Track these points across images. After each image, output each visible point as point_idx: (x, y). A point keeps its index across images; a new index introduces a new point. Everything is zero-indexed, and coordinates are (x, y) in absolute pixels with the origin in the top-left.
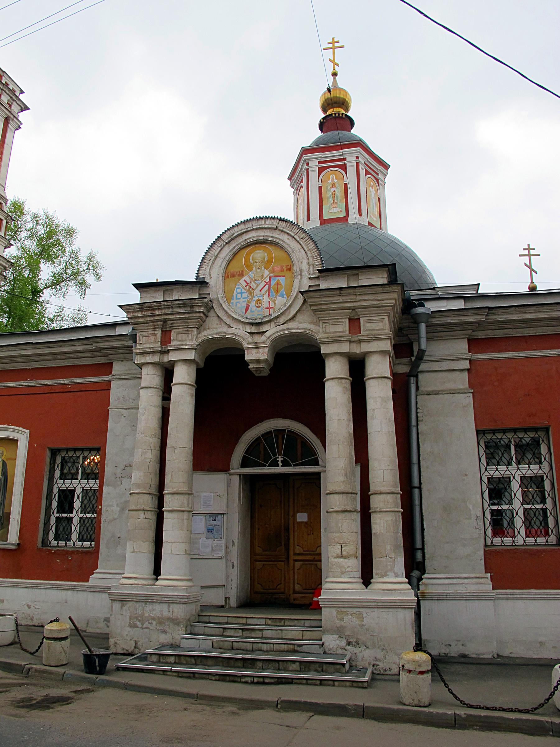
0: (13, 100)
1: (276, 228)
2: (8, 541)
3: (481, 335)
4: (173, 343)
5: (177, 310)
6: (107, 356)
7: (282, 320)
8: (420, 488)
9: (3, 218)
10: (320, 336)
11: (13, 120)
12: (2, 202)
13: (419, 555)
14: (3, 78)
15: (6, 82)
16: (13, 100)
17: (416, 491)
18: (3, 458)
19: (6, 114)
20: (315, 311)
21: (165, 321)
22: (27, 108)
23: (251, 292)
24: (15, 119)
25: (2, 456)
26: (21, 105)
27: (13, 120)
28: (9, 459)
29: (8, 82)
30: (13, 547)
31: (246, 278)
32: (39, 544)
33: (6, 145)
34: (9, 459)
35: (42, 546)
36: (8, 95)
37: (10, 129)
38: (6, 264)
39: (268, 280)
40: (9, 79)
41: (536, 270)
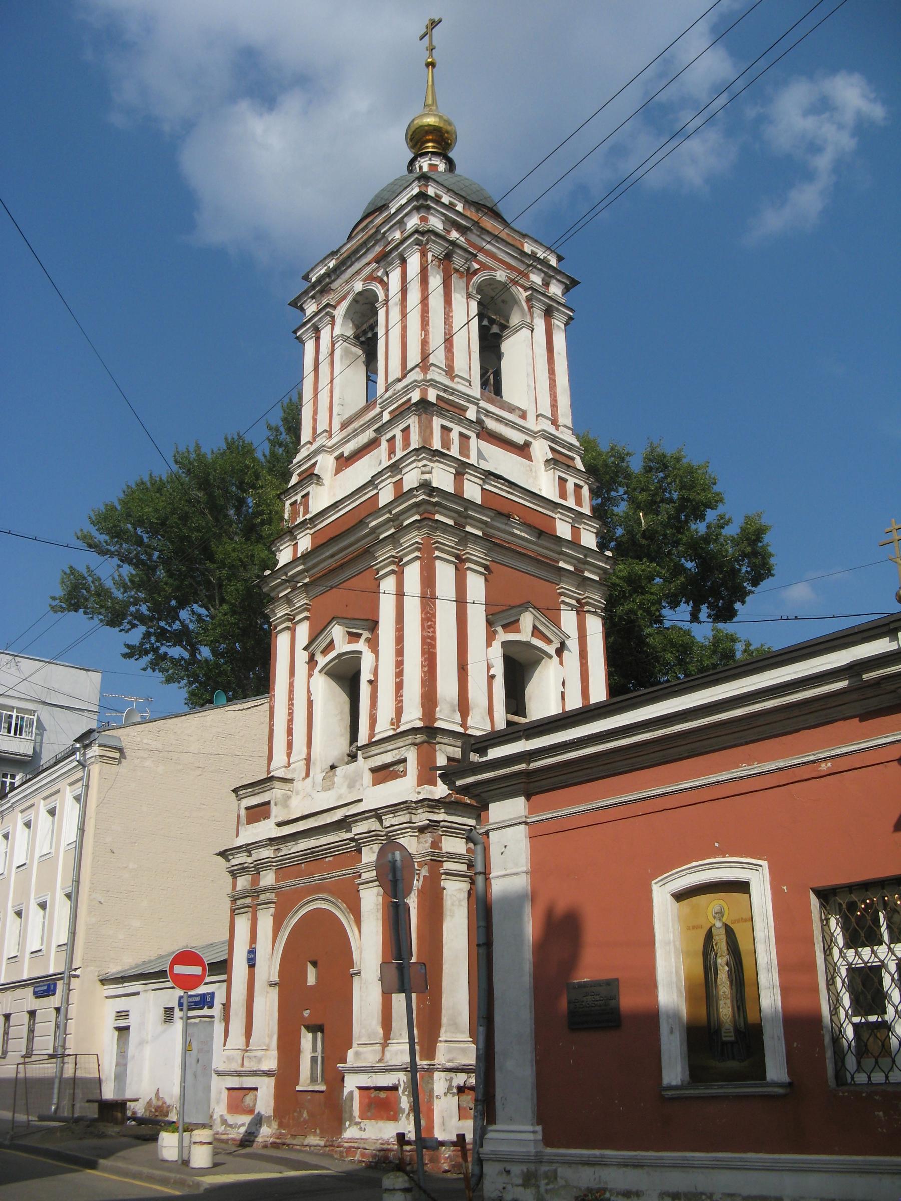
2: (768, 1079)
6: (895, 691)
11: (558, 310)
12: (575, 456)
15: (532, 251)
18: (724, 920)
19: (544, 303)
25: (723, 916)
27: (558, 310)
28: (738, 921)
30: (781, 1091)
32: (832, 1082)
34: (738, 921)
35: (838, 1085)
36: (540, 270)
37: (558, 326)
38: (606, 564)
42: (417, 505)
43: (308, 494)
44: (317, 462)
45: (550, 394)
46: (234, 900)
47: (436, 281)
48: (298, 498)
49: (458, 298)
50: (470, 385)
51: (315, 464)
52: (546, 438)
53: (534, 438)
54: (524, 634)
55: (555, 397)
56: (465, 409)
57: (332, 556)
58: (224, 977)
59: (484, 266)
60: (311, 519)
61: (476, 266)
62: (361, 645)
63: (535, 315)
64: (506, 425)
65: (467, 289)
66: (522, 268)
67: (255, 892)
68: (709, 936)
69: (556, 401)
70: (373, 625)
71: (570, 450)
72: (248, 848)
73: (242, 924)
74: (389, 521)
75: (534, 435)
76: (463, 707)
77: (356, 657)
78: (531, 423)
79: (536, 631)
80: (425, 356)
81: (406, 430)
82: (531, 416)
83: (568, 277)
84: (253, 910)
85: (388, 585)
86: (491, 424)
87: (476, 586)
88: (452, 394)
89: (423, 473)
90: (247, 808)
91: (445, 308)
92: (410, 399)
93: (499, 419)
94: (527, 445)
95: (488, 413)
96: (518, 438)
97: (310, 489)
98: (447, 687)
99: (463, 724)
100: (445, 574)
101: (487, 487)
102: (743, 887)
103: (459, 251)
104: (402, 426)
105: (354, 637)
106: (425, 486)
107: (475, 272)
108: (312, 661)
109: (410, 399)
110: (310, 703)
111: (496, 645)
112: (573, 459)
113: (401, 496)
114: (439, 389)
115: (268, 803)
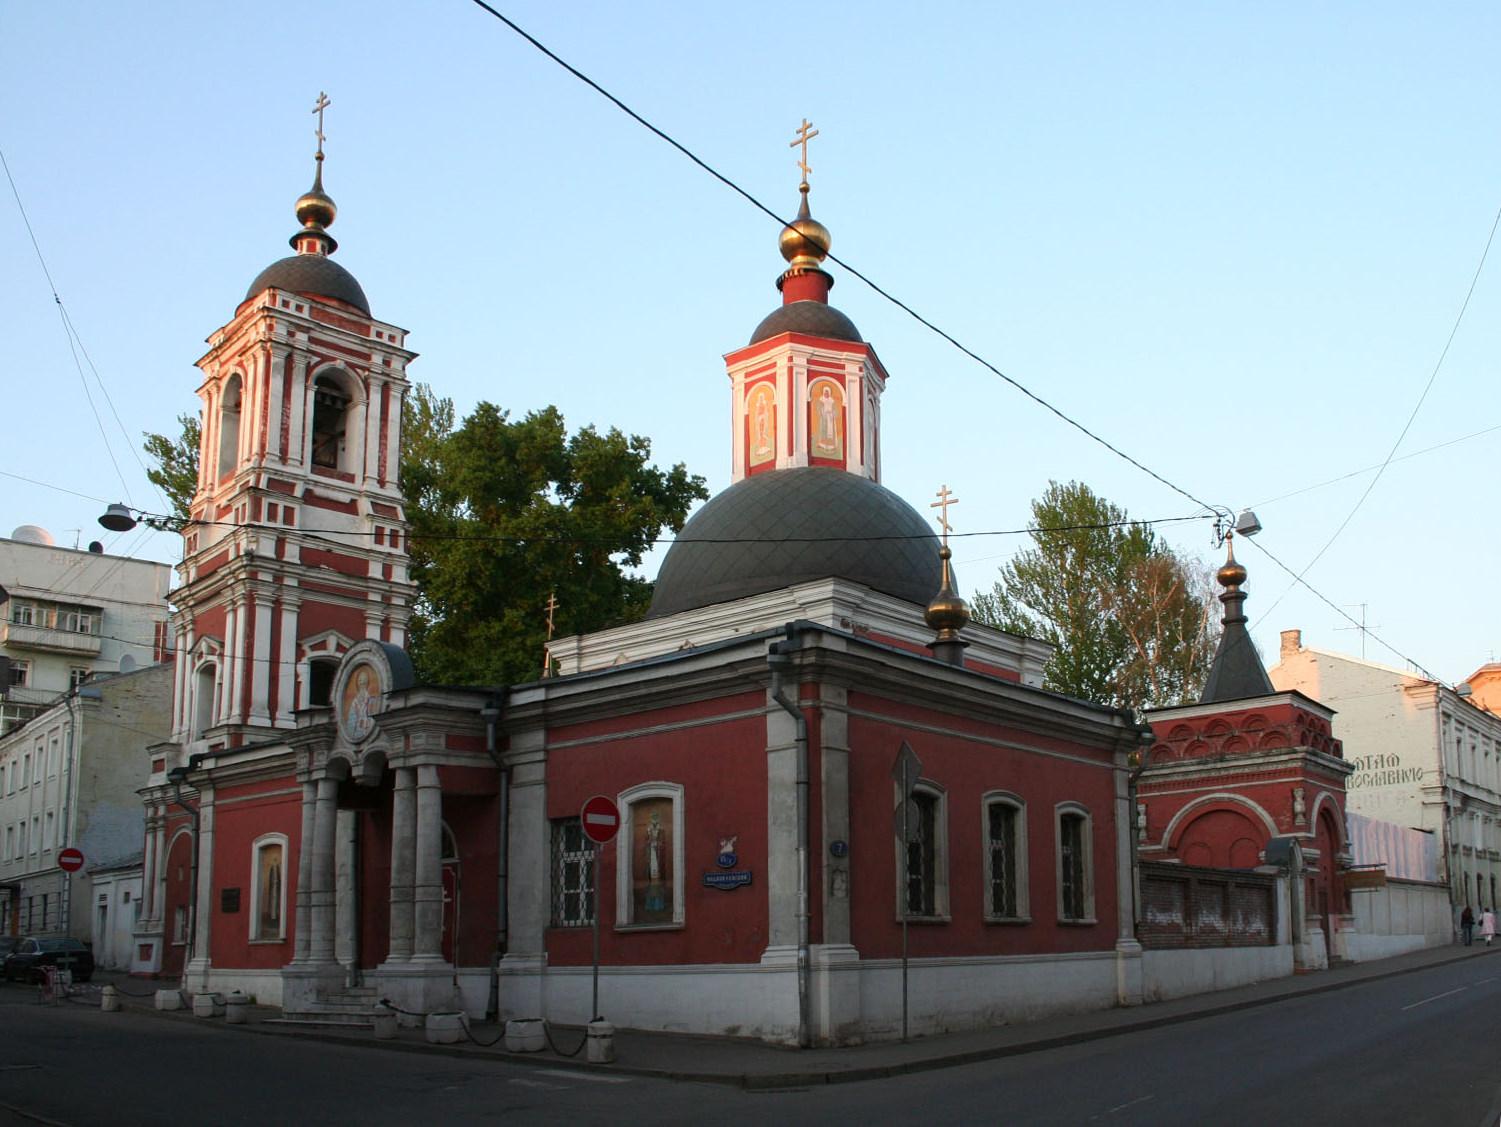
0: (392, 354)
1: (370, 651)
3: (557, 723)
4: (316, 764)
5: (311, 735)
7: (370, 740)
8: (506, 876)
9: (397, 528)
10: (389, 753)
11: (394, 383)
12: (395, 505)
13: (501, 936)
14: (372, 328)
16: (392, 354)
17: (501, 880)
20: (385, 731)
21: (308, 744)
22: (414, 355)
23: (357, 713)
24: (397, 381)
26: (405, 355)
29: (380, 330)
30: (281, 942)
31: (356, 700)
33: (390, 423)
37: (395, 397)
39: (366, 701)
40: (380, 325)
41: (939, 522)
42: (244, 566)
43: (195, 535)
44: (203, 510)
45: (379, 457)
46: (147, 823)
47: (277, 383)
48: (192, 535)
49: (297, 389)
50: (302, 464)
51: (203, 510)
52: (369, 497)
53: (360, 496)
54: (331, 651)
55: (385, 458)
56: (293, 485)
57: (204, 589)
58: (141, 874)
59: (324, 358)
60: (196, 557)
61: (317, 359)
62: (214, 658)
63: (371, 392)
64: (334, 490)
65: (306, 381)
66: (365, 350)
67: (154, 820)
68: (272, 870)
69: (385, 462)
70: (222, 645)
71: (391, 502)
72: (151, 790)
73: (150, 838)
74: (230, 573)
75: (359, 493)
76: (273, 704)
77: (213, 667)
78: (358, 485)
79: (340, 648)
80: (263, 446)
81: (244, 505)
82: (359, 479)
83: (408, 352)
84: (154, 830)
85: (230, 618)
86: (319, 491)
87: (289, 622)
88: (282, 475)
89: (251, 542)
90: (155, 762)
91: (283, 401)
92: (248, 481)
93: (327, 486)
94: (353, 502)
95: (316, 483)
96: (345, 498)
97: (198, 531)
98: (260, 693)
99: (273, 718)
100: (263, 616)
101: (305, 545)
102: (279, 846)
103: (299, 352)
104: (243, 502)
105: (212, 651)
106: (250, 555)
107: (317, 364)
108: (194, 664)
109: (248, 481)
110: (192, 693)
111: (305, 660)
112: (395, 508)
113: (238, 556)
114: (270, 473)
115: (162, 760)
